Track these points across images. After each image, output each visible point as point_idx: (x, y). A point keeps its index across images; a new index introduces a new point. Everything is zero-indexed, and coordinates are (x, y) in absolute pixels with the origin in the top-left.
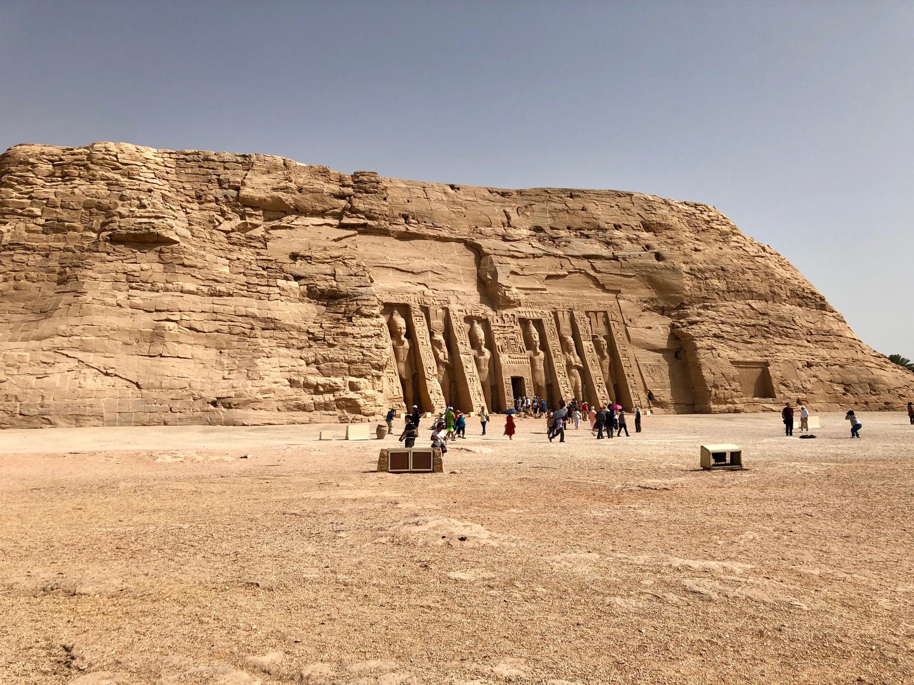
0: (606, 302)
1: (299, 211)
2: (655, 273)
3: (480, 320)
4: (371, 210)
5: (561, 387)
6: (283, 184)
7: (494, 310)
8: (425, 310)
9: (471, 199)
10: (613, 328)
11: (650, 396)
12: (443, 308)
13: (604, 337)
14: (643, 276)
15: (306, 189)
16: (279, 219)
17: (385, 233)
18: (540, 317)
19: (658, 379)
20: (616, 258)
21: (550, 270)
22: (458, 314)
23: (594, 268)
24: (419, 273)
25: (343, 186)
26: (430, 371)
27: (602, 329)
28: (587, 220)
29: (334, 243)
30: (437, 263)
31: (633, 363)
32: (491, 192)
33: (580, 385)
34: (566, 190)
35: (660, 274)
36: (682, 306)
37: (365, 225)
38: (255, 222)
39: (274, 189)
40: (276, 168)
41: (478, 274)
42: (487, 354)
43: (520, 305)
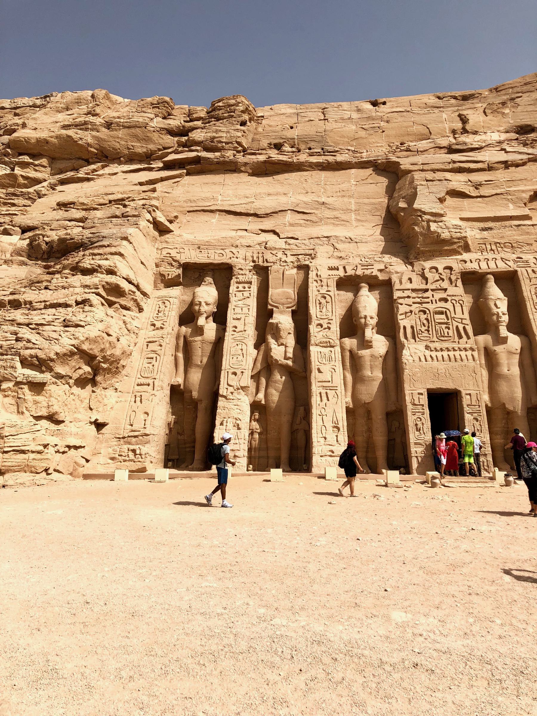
1: (106, 156)
3: (374, 284)
4: (214, 138)
6: (82, 119)
7: (408, 261)
8: (262, 271)
9: (401, 110)
12: (300, 267)
15: (118, 124)
16: (76, 170)
17: (230, 168)
18: (513, 266)
22: (324, 273)
24: (267, 215)
25: (191, 121)
26: (234, 381)
29: (139, 188)
30: (305, 199)
32: (439, 98)
37: (197, 160)
38: (32, 174)
39: (65, 127)
40: (78, 102)
41: (388, 207)
42: (380, 344)
43: (467, 248)
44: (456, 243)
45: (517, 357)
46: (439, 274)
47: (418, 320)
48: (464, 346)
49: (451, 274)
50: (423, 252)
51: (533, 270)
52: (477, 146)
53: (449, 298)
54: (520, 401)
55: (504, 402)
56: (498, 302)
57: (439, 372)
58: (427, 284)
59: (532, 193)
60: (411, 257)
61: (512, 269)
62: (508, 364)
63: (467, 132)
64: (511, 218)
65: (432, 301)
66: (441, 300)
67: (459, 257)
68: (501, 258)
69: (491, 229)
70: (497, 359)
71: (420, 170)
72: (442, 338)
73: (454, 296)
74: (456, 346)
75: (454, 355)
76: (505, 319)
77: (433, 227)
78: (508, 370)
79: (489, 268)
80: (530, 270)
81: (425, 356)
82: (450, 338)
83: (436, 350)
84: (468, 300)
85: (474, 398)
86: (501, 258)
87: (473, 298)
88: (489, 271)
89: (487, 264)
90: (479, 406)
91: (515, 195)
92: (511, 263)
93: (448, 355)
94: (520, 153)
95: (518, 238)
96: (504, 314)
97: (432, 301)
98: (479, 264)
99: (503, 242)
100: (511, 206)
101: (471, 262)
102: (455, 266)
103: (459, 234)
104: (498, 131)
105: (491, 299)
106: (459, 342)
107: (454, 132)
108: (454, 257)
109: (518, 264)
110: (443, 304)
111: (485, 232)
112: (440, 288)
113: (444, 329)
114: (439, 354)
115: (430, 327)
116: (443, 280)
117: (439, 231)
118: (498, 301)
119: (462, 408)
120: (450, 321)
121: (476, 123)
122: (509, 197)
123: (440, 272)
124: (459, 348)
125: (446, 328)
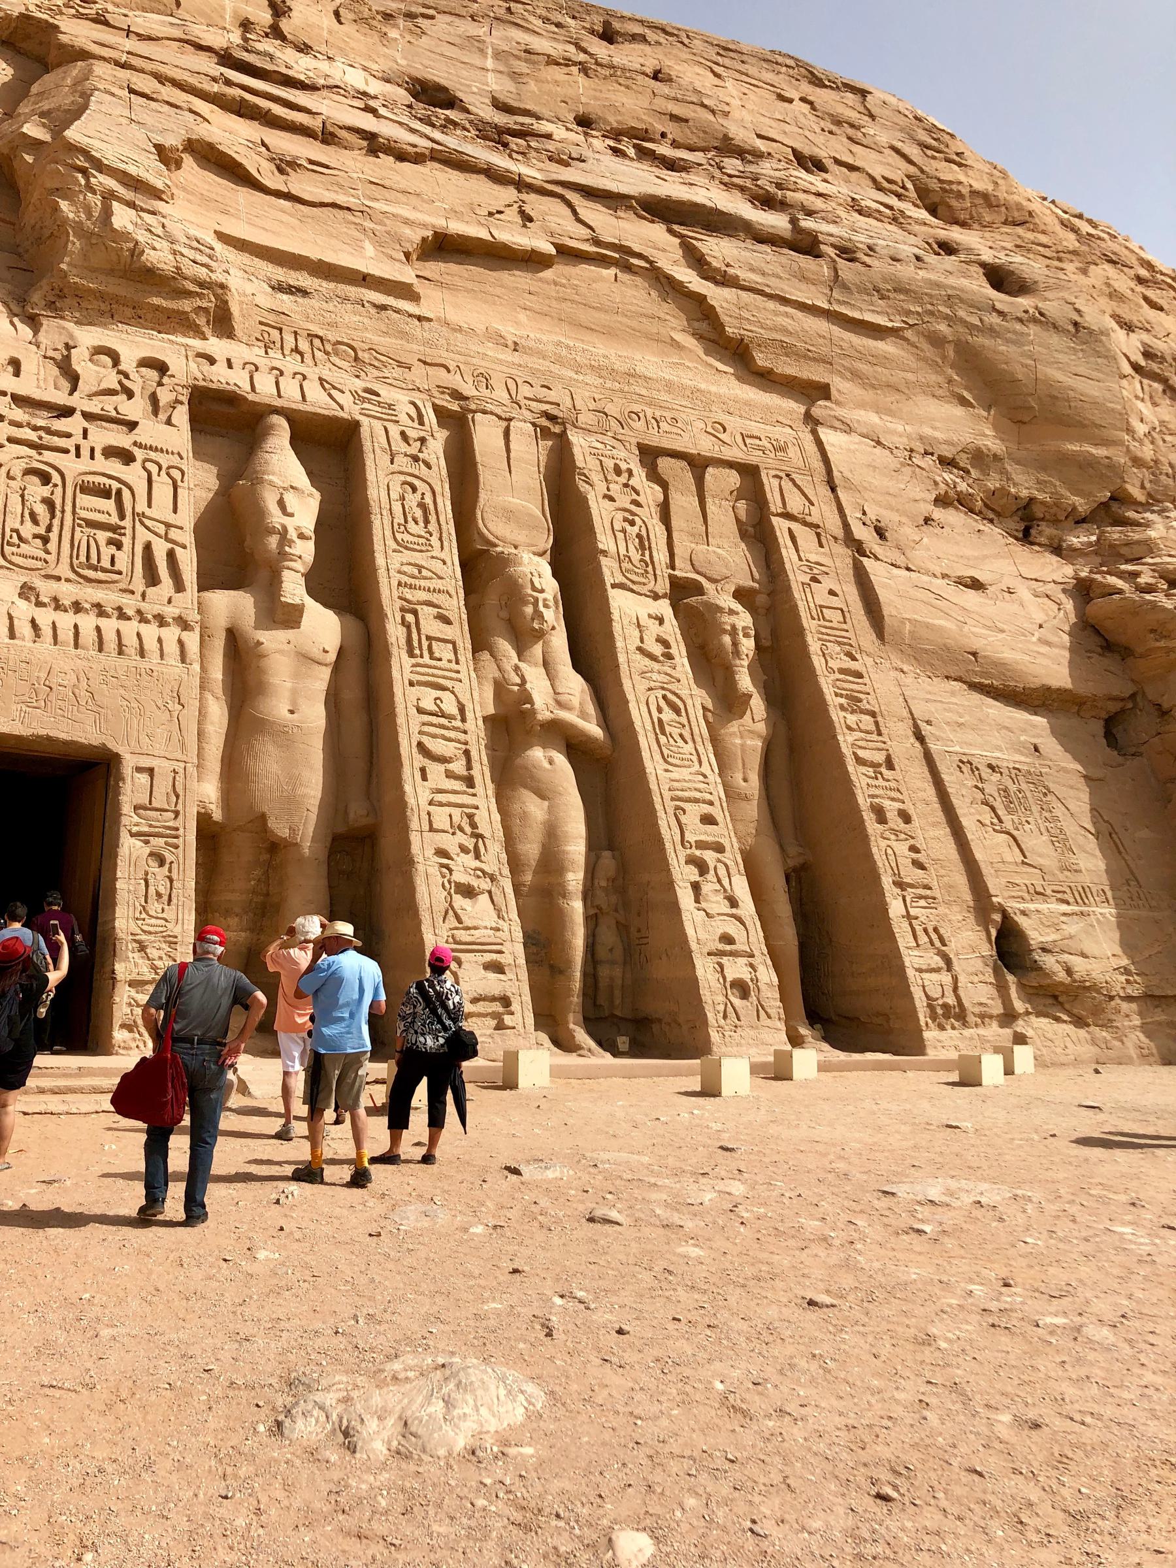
0: (754, 428)
2: (992, 331)
5: (421, 846)
10: (788, 553)
11: (1010, 949)
13: (740, 594)
14: (937, 341)
18: (350, 409)
19: (1037, 843)
20: (806, 245)
21: (454, 213)
23: (697, 261)
27: (727, 560)
28: (677, 109)
31: (904, 747)
33: (576, 847)
34: (589, 9)
35: (1019, 340)
36: (1113, 509)
43: (223, 323)
44: (189, 294)
45: (325, 673)
46: (119, 372)
47: (15, 500)
48: (157, 609)
49: (160, 384)
50: (80, 295)
51: (403, 434)
52: (302, 77)
53: (139, 454)
54: (315, 810)
55: (265, 809)
56: (290, 499)
57: (54, 681)
58: (71, 394)
59: (430, 233)
60: (36, 297)
61: (346, 416)
62: (295, 693)
63: (283, 38)
64: (364, 280)
65: (78, 448)
66: (111, 452)
67: (196, 344)
68: (320, 379)
69: (304, 293)
70: (261, 671)
71: (117, 63)
72: (91, 574)
73: (156, 450)
74: (130, 604)
75: (118, 631)
76: (305, 550)
77: (122, 218)
78: (292, 712)
79: (279, 396)
80: (395, 431)
81: (11, 618)
82: (116, 577)
83: (58, 606)
84: (202, 482)
85: (163, 786)
86: (320, 379)
87: (219, 476)
88: (278, 403)
89: (277, 383)
90: (177, 813)
91: (381, 223)
92: (346, 399)
93: (98, 629)
94: (413, 131)
95: (376, 339)
96: (302, 536)
97: (78, 448)
98: (251, 378)
99: (333, 339)
100: (369, 249)
101: (230, 366)
102: (176, 364)
103: (204, 270)
104: (365, 69)
105: (271, 484)
106: (144, 595)
107: (246, 25)
108: (180, 339)
109: (366, 405)
110: (114, 467)
111: (285, 297)
112: (114, 414)
113: (102, 543)
114: (66, 621)
115: (56, 529)
116: (130, 394)
117: (141, 239)
118: (291, 496)
119: (118, 815)
120: (127, 523)
121: (309, 25)
122: (368, 224)
123: (122, 367)
124: (139, 612)
125: (110, 542)
